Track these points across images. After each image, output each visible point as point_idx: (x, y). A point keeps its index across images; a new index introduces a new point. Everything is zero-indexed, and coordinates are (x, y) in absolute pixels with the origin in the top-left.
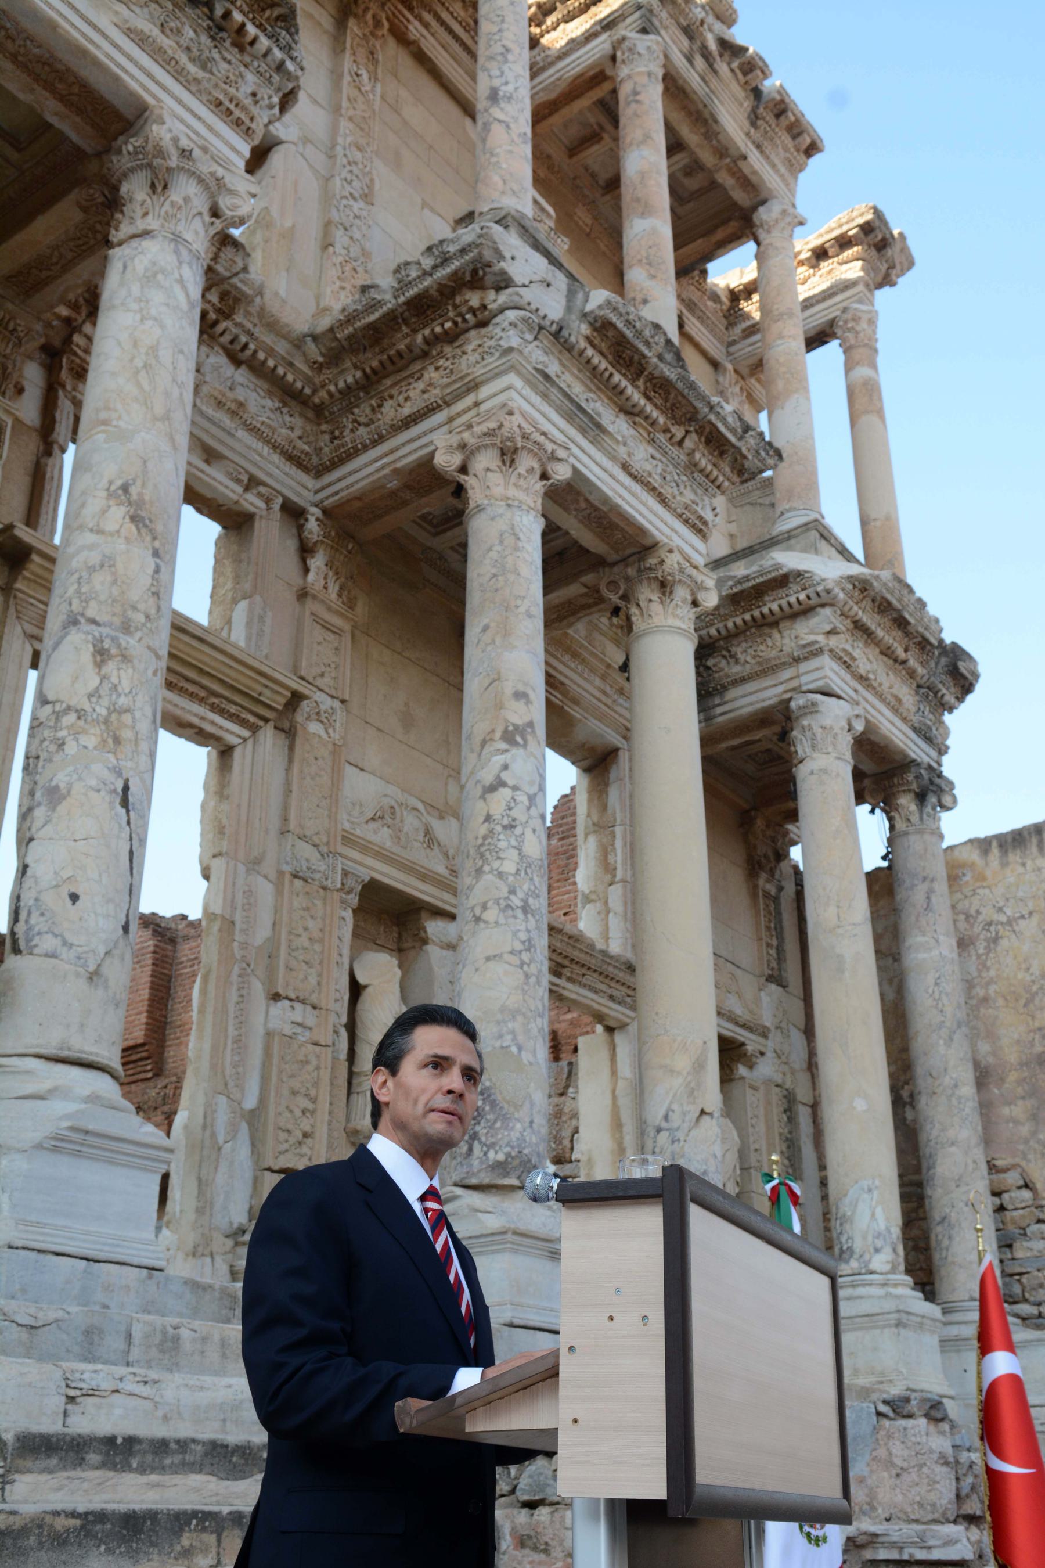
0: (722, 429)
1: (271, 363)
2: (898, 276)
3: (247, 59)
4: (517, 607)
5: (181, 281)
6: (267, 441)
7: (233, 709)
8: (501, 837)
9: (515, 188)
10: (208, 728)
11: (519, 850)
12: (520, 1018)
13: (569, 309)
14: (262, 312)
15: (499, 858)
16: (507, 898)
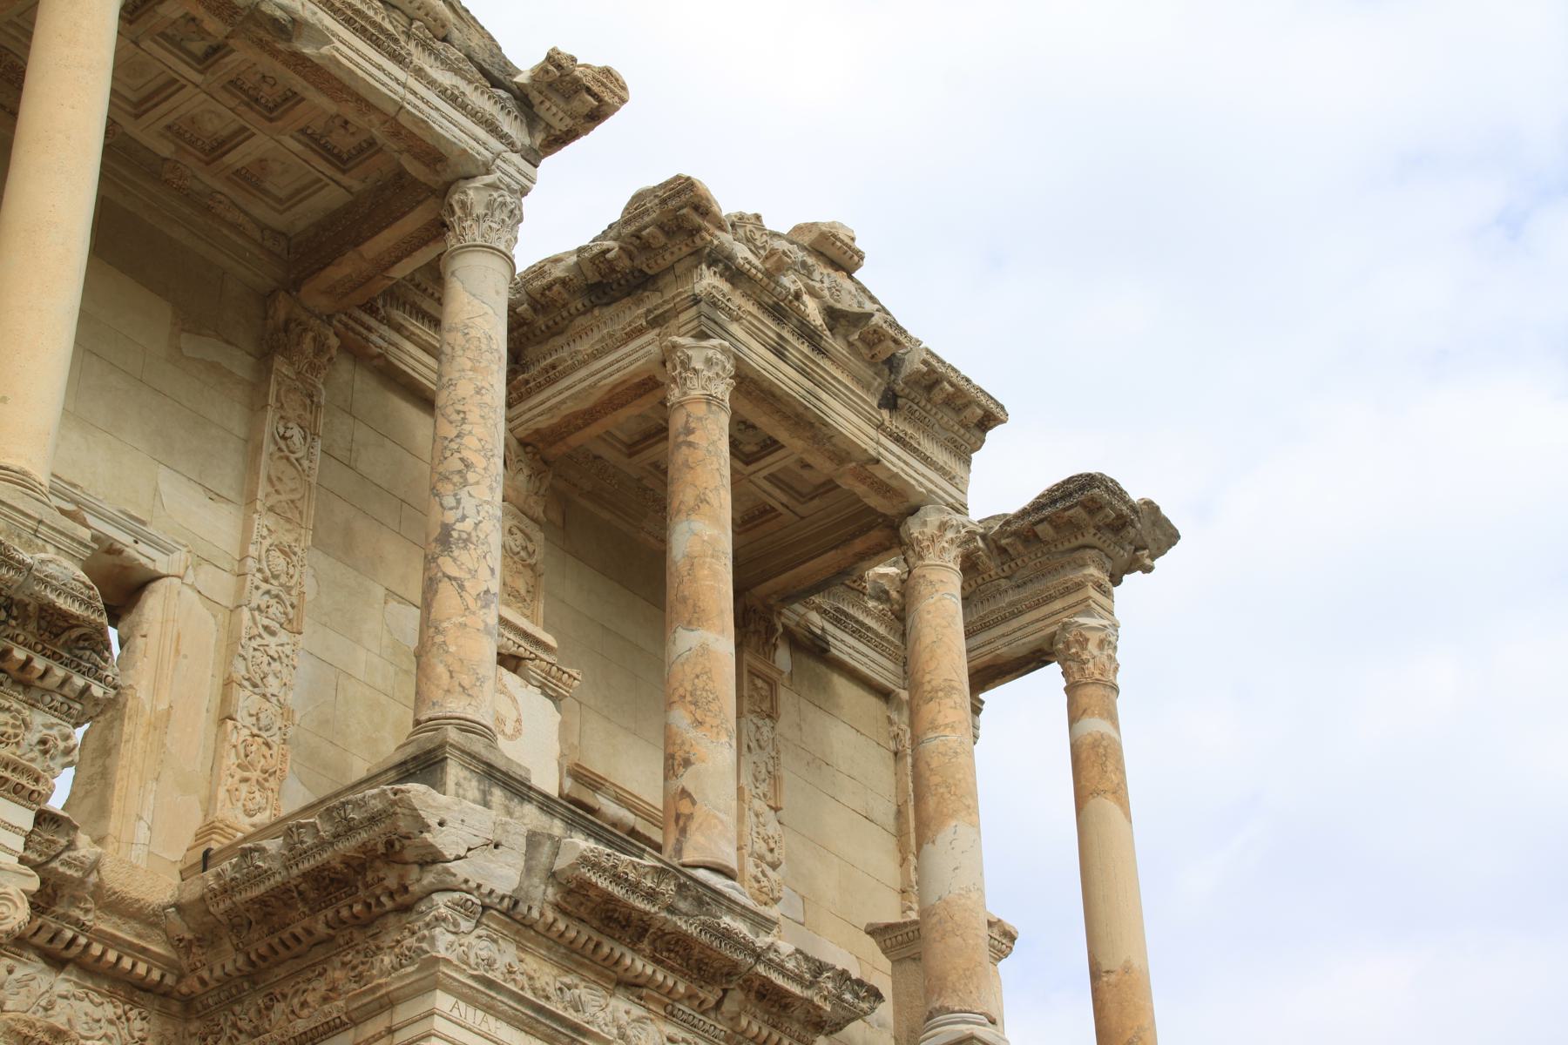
0: (779, 981)
2: (1153, 557)
3: (36, 694)
9: (466, 683)
13: (528, 871)
14: (98, 891)
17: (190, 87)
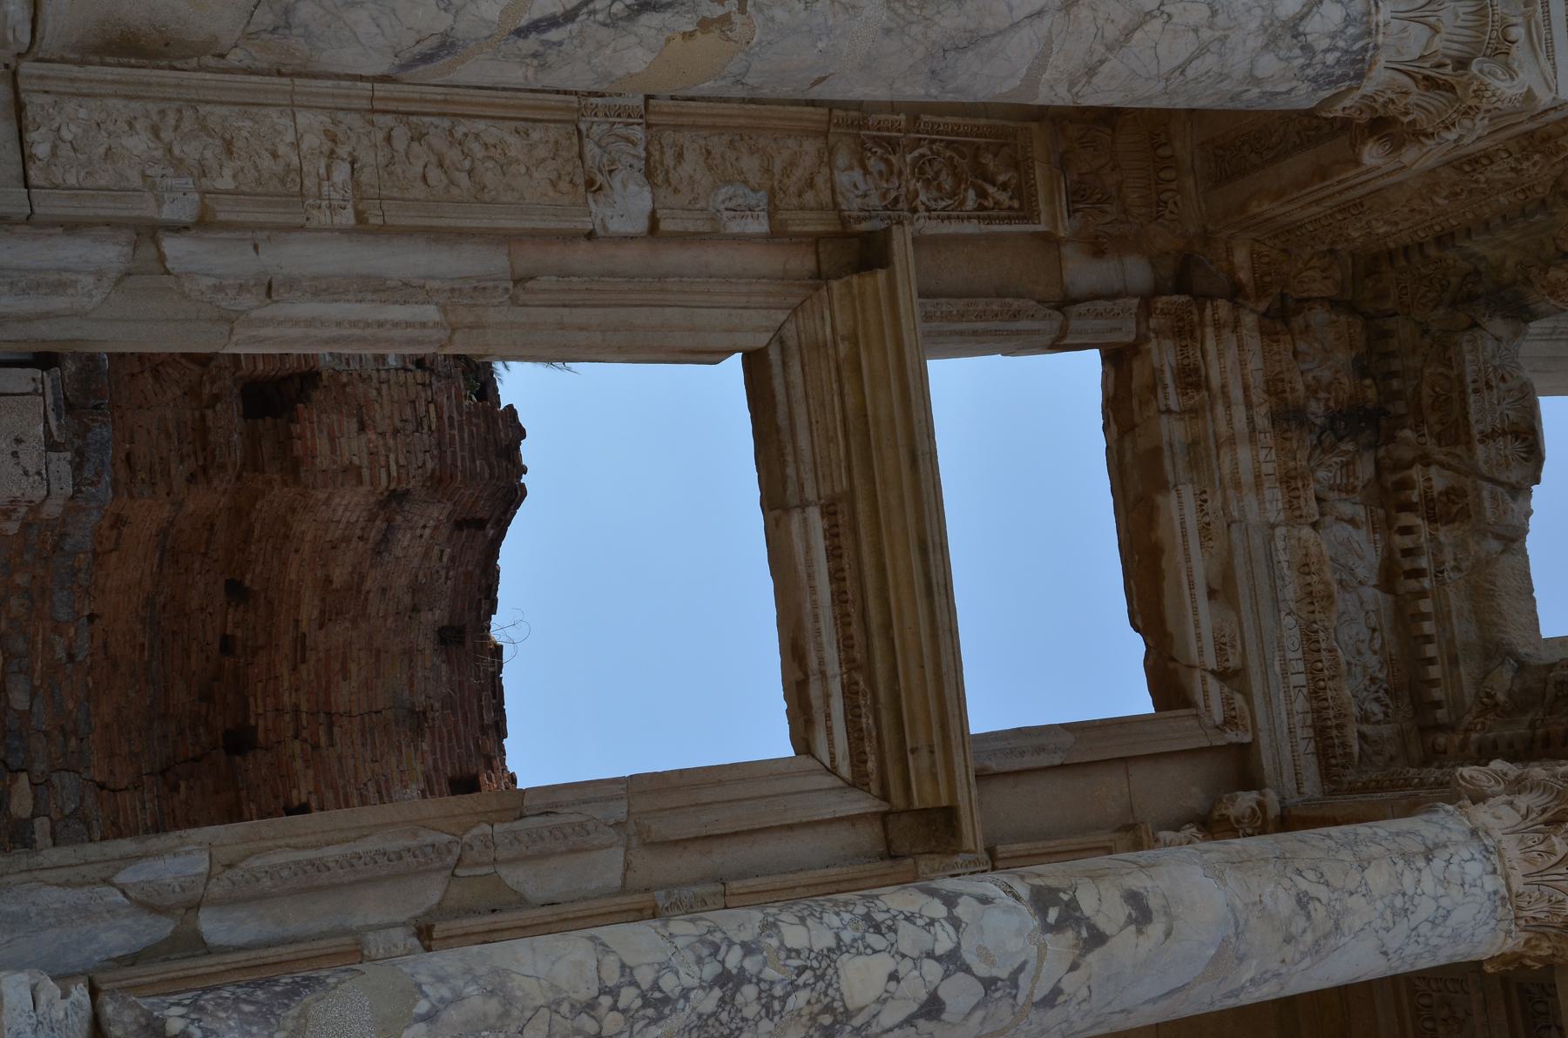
1: (1428, 627)
4: (1299, 872)
6: (1313, 673)
7: (867, 721)
8: (847, 917)
10: (815, 691)
11: (840, 947)
12: (493, 1006)
15: (802, 920)
16: (731, 944)
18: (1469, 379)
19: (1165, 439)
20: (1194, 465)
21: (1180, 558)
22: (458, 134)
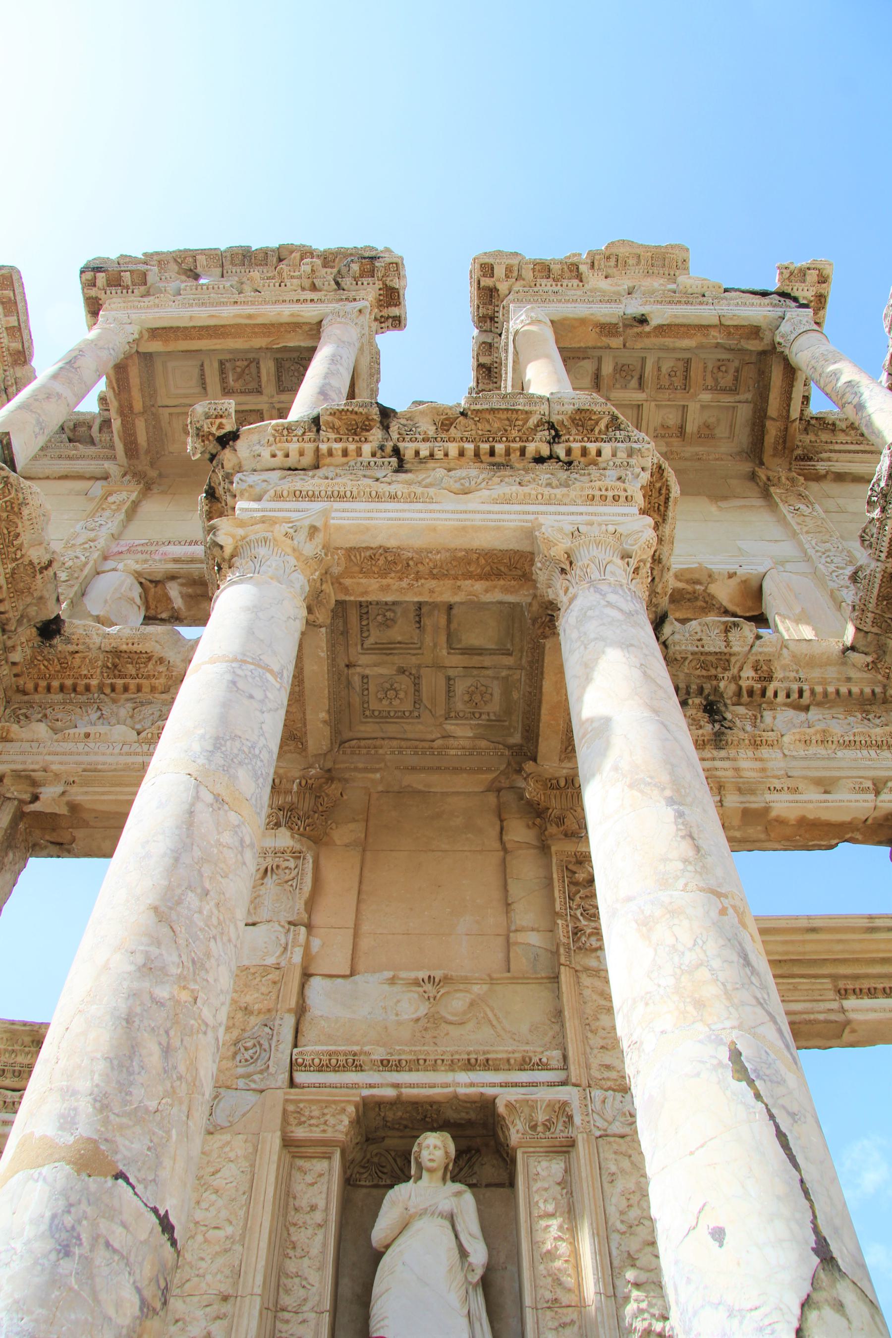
1: (831, 689)
5: (609, 604)
6: (868, 746)
17: (645, 404)
18: (696, 649)
19: (738, 805)
20: (752, 792)
21: (810, 806)
22: (622, 1227)
